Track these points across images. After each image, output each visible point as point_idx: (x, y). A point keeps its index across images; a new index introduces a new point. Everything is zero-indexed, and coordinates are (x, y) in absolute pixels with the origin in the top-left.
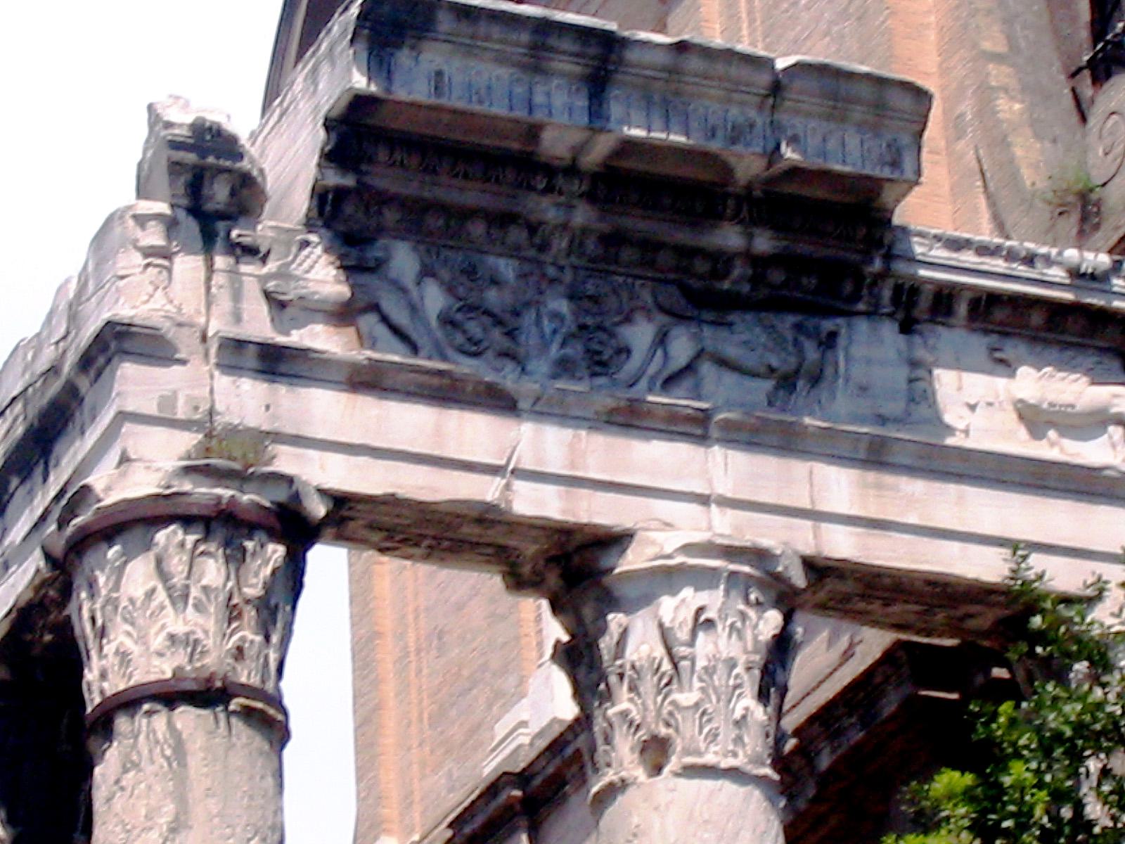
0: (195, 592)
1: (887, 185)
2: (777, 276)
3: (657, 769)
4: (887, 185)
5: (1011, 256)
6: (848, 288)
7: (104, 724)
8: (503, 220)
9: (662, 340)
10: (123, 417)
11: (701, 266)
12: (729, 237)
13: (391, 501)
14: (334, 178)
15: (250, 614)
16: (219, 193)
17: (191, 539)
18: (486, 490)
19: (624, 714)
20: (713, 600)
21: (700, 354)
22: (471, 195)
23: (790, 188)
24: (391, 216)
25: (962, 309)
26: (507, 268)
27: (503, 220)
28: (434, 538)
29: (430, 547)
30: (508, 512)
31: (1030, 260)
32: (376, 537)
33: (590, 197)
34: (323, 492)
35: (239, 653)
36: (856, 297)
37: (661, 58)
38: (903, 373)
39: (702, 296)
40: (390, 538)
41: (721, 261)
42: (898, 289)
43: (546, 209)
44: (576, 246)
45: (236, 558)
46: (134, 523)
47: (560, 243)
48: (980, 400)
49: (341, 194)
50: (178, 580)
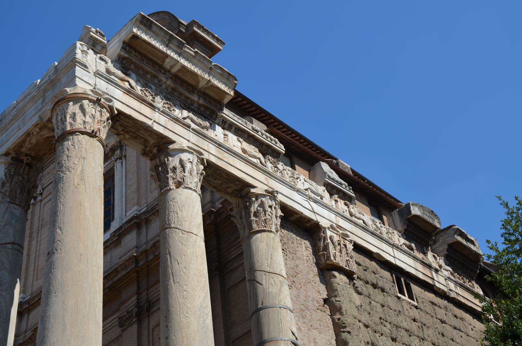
1: (227, 95)
2: (202, 109)
3: (177, 188)
4: (227, 95)
6: (214, 117)
8: (155, 77)
11: (189, 102)
12: (195, 98)
13: (129, 117)
14: (123, 54)
16: (99, 48)
17: (90, 104)
18: (150, 123)
21: (188, 117)
23: (207, 92)
24: (132, 67)
25: (233, 129)
27: (155, 77)
28: (133, 133)
29: (131, 136)
32: (120, 129)
33: (172, 79)
34: (117, 109)
35: (99, 130)
36: (215, 119)
38: (223, 136)
40: (123, 130)
42: (223, 120)
44: (166, 88)
46: (77, 98)
47: (164, 86)
49: (124, 58)
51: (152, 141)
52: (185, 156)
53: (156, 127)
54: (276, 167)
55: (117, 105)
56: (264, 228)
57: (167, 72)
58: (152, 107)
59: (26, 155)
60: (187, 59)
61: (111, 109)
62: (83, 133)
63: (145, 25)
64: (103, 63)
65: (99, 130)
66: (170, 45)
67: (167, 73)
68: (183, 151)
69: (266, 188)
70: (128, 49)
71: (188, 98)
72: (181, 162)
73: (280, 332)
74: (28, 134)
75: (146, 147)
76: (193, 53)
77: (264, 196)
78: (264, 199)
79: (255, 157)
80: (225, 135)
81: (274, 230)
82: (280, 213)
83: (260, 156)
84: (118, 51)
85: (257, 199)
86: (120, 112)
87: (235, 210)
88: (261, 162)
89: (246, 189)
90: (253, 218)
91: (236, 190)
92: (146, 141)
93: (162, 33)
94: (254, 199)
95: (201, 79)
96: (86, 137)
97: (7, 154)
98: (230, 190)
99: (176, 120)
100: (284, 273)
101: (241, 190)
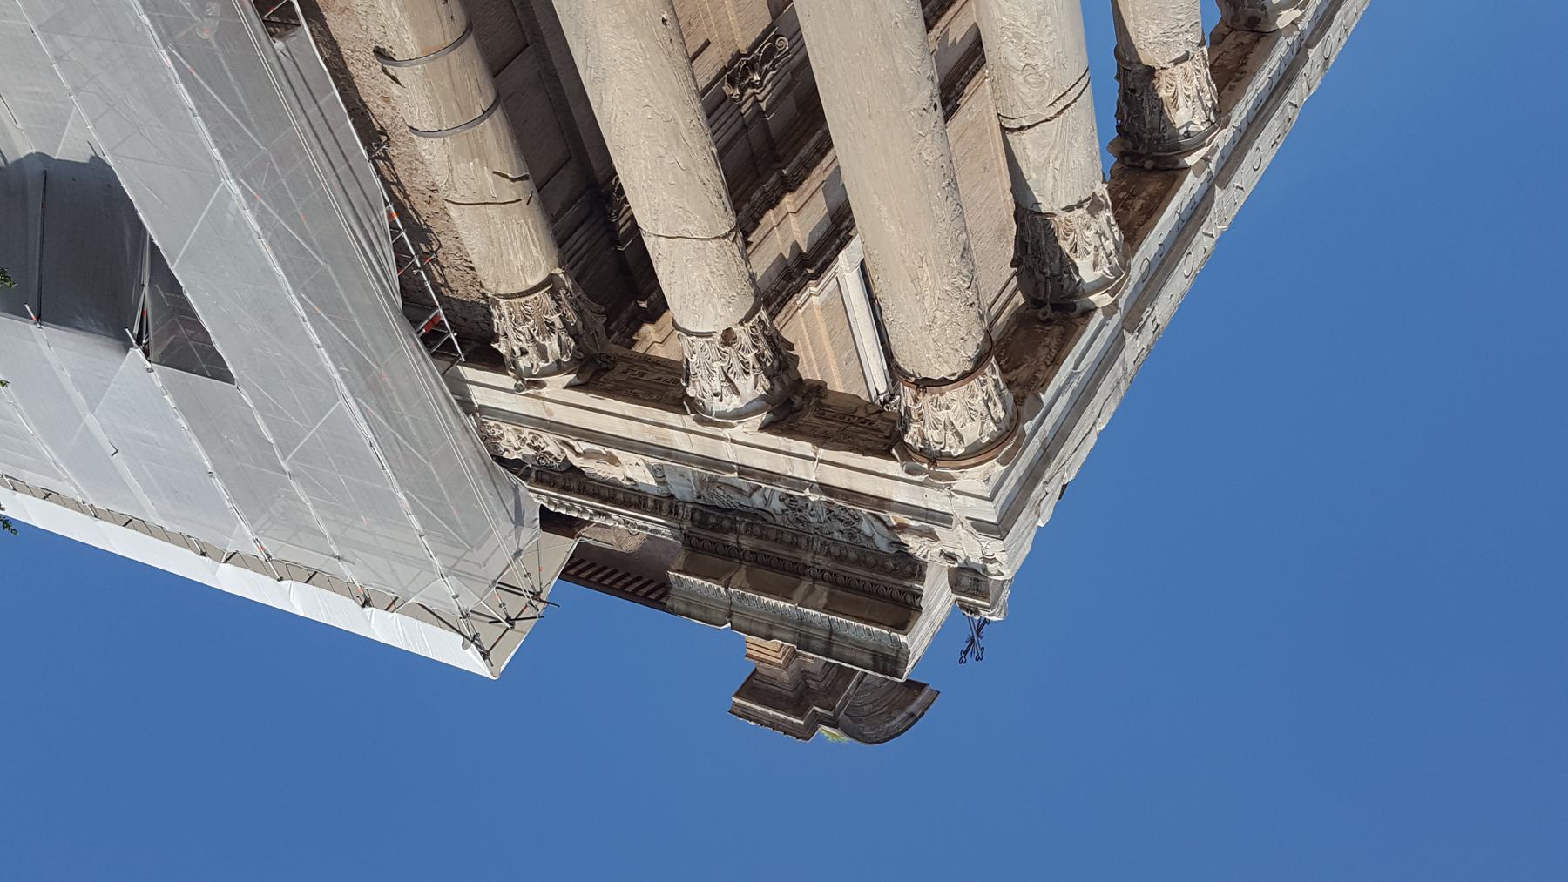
0: (941, 427)
2: (726, 523)
3: (729, 330)
5: (634, 525)
6: (697, 515)
7: (979, 362)
8: (841, 559)
9: (767, 502)
10: (991, 499)
11: (757, 530)
12: (745, 542)
13: (865, 451)
15: (915, 417)
16: (966, 581)
18: (823, 453)
19: (748, 352)
20: (716, 406)
22: (857, 572)
24: (890, 564)
25: (650, 503)
26: (837, 535)
27: (841, 559)
30: (814, 444)
31: (626, 523)
32: (879, 424)
33: (806, 566)
34: (894, 459)
35: (916, 400)
36: (694, 510)
37: (775, 633)
38: (668, 479)
39: (757, 517)
41: (749, 533)
43: (824, 563)
45: (925, 440)
46: (978, 453)
47: (817, 545)
48: (634, 470)
50: (949, 433)
51: (809, 417)
52: (732, 403)
53: (806, 448)
54: (537, 448)
55: (894, 468)
56: (523, 300)
57: (820, 578)
58: (825, 488)
59: (1049, 322)
60: (783, 616)
61: (907, 453)
62: (944, 382)
63: (886, 658)
64: (948, 550)
65: (916, 400)
66: (825, 635)
67: (819, 575)
68: (739, 415)
69: (544, 392)
70: (909, 598)
71: (760, 537)
72: (737, 393)
73: (424, 75)
74: (1056, 362)
75: (819, 404)
76: (775, 633)
77: (546, 373)
78: (543, 364)
79: (585, 455)
80: (664, 483)
81: (502, 301)
82: (502, 348)
83: (577, 462)
84: (925, 588)
85: (558, 361)
86: (886, 454)
87: (600, 328)
88: (572, 448)
89: (587, 377)
90: (555, 318)
91: (607, 370)
92: (821, 415)
93: (848, 653)
94: (565, 360)
95: (745, 584)
96: (935, 375)
97: (1088, 312)
98: (621, 366)
99: (771, 477)
100: (453, 211)
101: (600, 372)
